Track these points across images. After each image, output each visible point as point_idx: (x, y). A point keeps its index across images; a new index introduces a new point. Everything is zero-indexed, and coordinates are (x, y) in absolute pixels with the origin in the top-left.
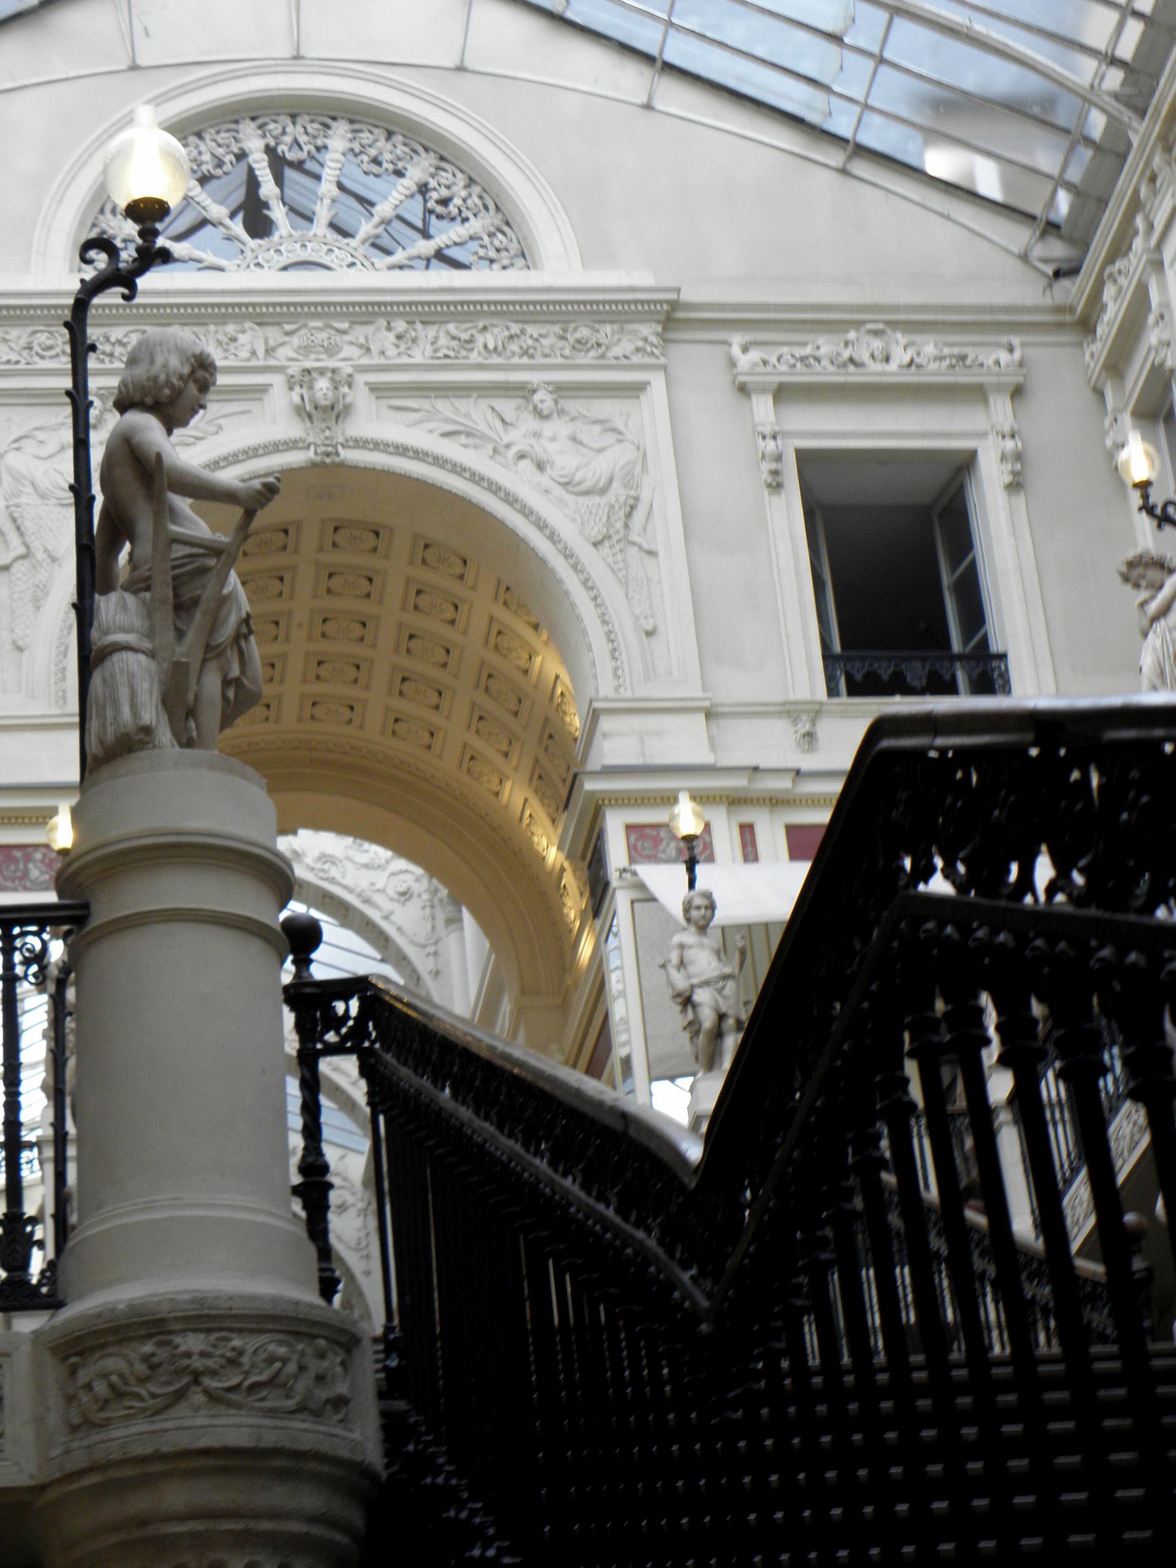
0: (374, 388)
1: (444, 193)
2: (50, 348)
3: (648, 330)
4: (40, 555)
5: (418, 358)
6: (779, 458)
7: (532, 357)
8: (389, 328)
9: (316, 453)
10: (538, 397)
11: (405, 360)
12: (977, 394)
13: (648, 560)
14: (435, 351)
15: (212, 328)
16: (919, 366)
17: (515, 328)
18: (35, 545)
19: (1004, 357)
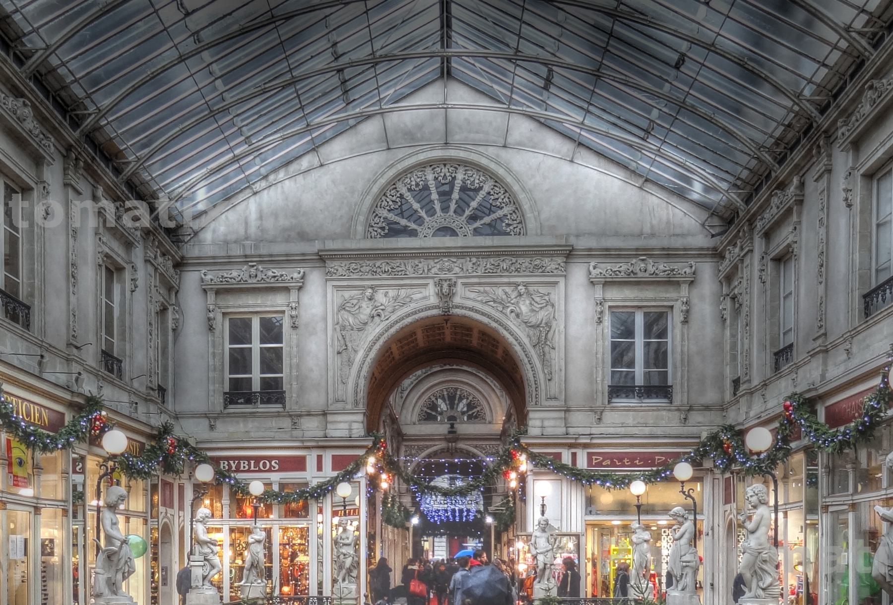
0: (464, 284)
1: (496, 196)
2: (356, 269)
3: (560, 260)
4: (350, 348)
5: (479, 274)
6: (601, 312)
7: (519, 272)
8: (470, 261)
9: (443, 311)
10: (520, 288)
11: (475, 274)
12: (678, 284)
13: (552, 351)
14: (486, 270)
15: (410, 261)
16: (657, 274)
17: (514, 260)
18: (349, 345)
19: (688, 270)
